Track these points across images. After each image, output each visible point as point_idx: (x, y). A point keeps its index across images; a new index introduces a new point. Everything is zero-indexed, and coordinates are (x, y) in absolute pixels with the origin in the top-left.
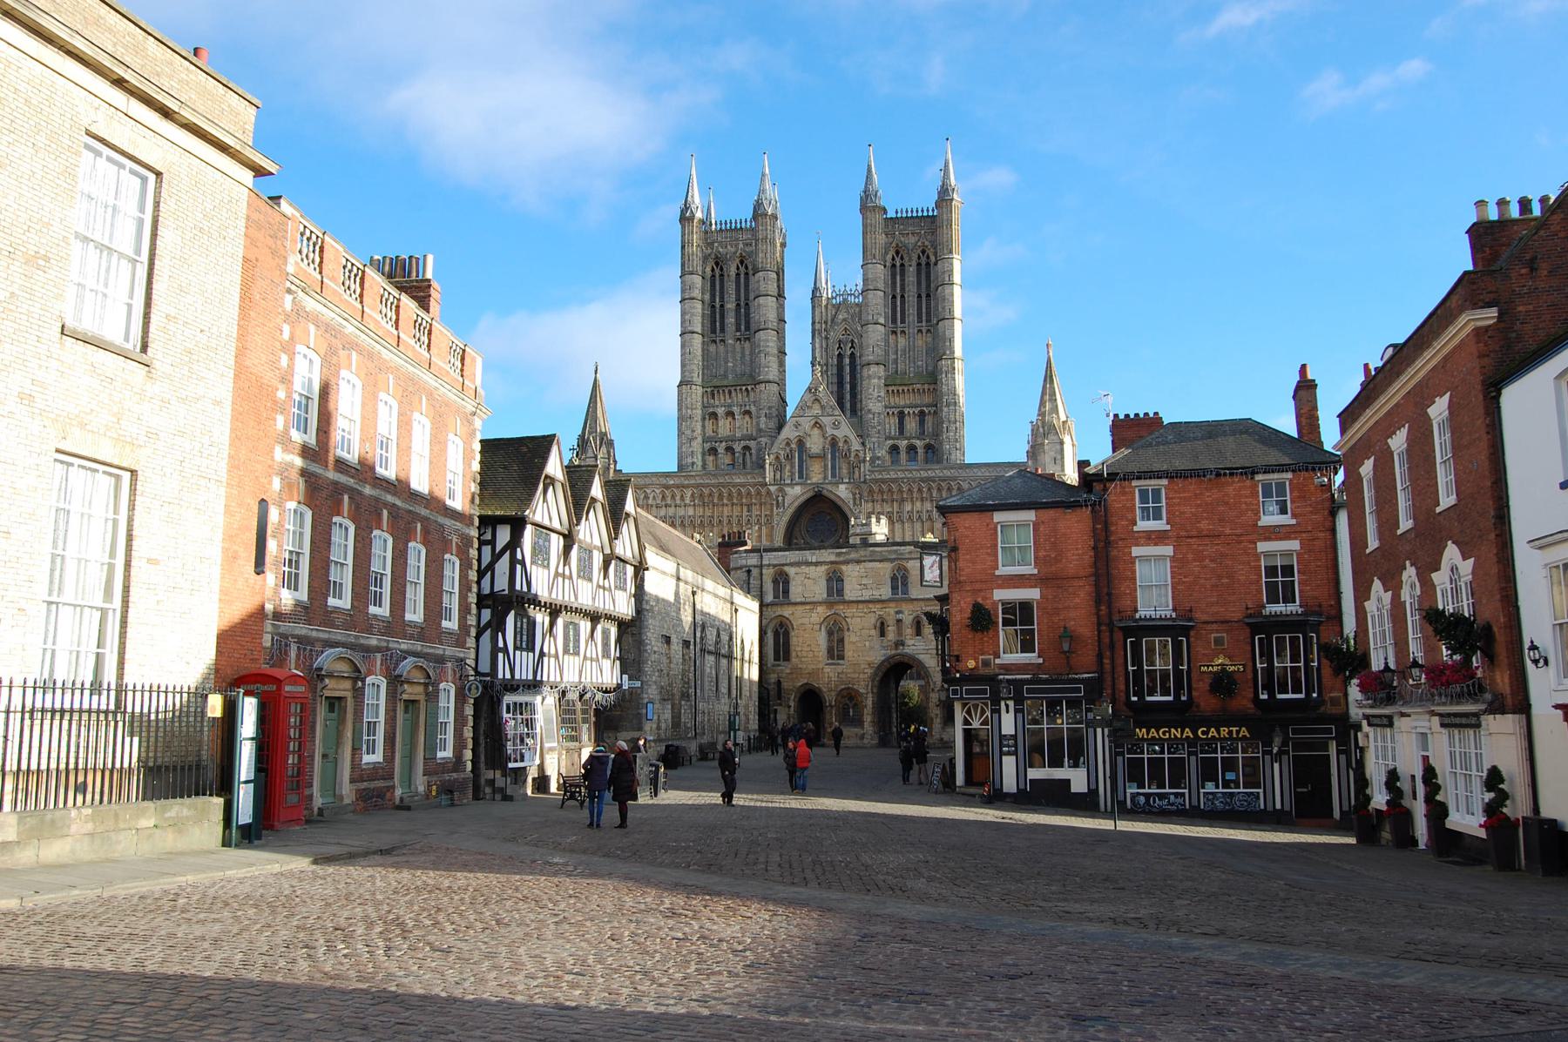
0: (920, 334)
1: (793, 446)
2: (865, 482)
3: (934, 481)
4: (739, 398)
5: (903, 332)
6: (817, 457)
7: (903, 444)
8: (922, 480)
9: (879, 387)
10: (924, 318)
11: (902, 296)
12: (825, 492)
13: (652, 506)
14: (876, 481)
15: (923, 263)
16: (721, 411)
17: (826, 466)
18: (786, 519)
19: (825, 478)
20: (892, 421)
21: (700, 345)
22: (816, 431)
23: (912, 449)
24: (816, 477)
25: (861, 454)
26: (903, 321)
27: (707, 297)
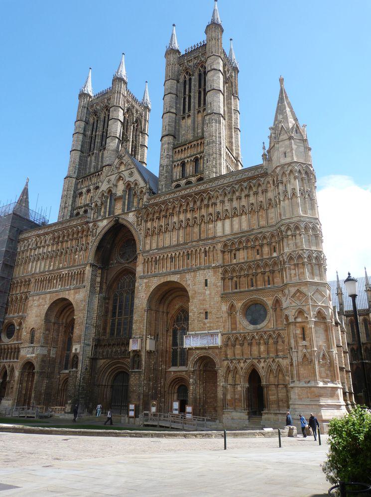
0: (199, 114)
2: (145, 208)
4: (94, 180)
5: (189, 116)
6: (120, 198)
7: (183, 182)
9: (168, 149)
10: (202, 102)
12: (120, 220)
13: (31, 249)
14: (153, 205)
15: (202, 73)
17: (124, 203)
18: (96, 244)
19: (123, 210)
21: (78, 157)
22: (121, 182)
25: (144, 190)
26: (189, 110)
27: (89, 133)
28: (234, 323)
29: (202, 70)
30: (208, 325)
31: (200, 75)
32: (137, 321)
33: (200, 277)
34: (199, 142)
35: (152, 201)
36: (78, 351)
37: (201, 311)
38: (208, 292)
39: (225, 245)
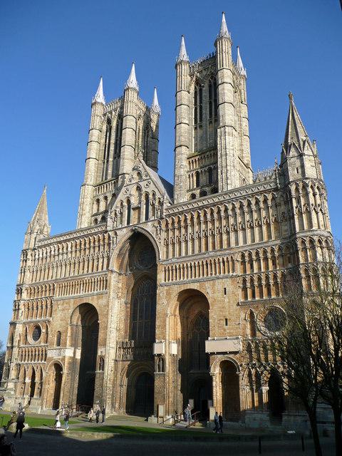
1: (125, 204)
3: (207, 208)
6: (138, 208)
7: (197, 192)
8: (200, 208)
10: (213, 114)
11: (201, 107)
12: (140, 230)
14: (169, 216)
16: (101, 198)
20: (191, 180)
23: (203, 194)
24: (134, 221)
25: (161, 200)
26: (201, 120)
27: (103, 141)
28: (254, 330)
29: (212, 81)
30: (228, 331)
31: (210, 86)
32: (160, 326)
33: (219, 285)
34: (212, 152)
35: (171, 212)
36: (103, 354)
37: (222, 318)
38: (226, 300)
39: (243, 256)
